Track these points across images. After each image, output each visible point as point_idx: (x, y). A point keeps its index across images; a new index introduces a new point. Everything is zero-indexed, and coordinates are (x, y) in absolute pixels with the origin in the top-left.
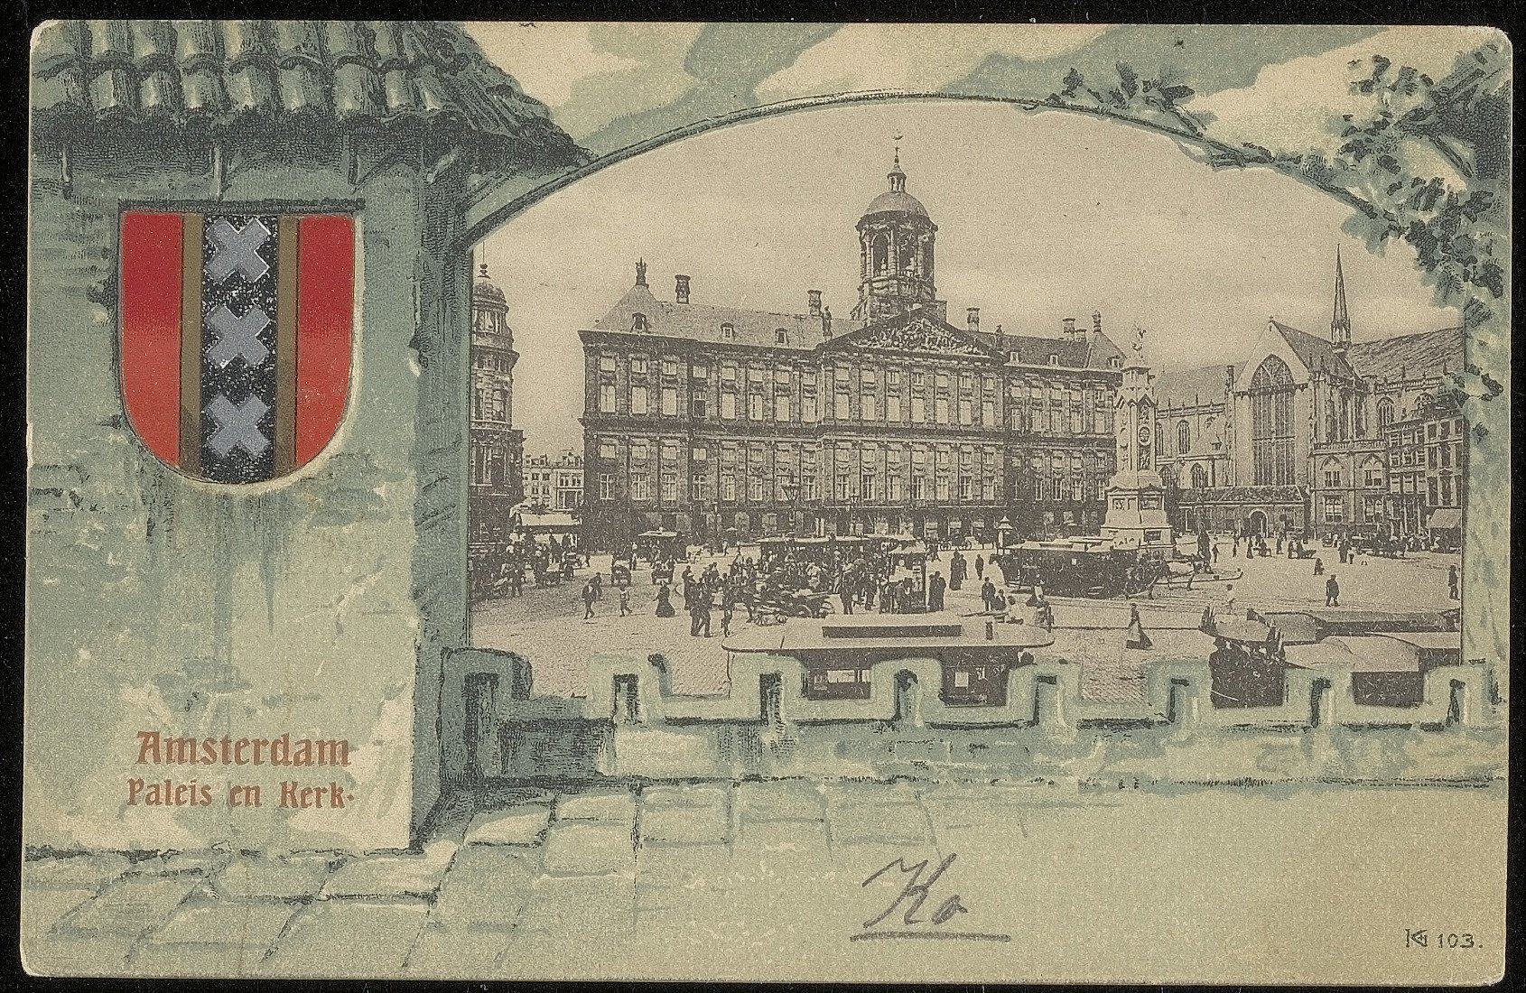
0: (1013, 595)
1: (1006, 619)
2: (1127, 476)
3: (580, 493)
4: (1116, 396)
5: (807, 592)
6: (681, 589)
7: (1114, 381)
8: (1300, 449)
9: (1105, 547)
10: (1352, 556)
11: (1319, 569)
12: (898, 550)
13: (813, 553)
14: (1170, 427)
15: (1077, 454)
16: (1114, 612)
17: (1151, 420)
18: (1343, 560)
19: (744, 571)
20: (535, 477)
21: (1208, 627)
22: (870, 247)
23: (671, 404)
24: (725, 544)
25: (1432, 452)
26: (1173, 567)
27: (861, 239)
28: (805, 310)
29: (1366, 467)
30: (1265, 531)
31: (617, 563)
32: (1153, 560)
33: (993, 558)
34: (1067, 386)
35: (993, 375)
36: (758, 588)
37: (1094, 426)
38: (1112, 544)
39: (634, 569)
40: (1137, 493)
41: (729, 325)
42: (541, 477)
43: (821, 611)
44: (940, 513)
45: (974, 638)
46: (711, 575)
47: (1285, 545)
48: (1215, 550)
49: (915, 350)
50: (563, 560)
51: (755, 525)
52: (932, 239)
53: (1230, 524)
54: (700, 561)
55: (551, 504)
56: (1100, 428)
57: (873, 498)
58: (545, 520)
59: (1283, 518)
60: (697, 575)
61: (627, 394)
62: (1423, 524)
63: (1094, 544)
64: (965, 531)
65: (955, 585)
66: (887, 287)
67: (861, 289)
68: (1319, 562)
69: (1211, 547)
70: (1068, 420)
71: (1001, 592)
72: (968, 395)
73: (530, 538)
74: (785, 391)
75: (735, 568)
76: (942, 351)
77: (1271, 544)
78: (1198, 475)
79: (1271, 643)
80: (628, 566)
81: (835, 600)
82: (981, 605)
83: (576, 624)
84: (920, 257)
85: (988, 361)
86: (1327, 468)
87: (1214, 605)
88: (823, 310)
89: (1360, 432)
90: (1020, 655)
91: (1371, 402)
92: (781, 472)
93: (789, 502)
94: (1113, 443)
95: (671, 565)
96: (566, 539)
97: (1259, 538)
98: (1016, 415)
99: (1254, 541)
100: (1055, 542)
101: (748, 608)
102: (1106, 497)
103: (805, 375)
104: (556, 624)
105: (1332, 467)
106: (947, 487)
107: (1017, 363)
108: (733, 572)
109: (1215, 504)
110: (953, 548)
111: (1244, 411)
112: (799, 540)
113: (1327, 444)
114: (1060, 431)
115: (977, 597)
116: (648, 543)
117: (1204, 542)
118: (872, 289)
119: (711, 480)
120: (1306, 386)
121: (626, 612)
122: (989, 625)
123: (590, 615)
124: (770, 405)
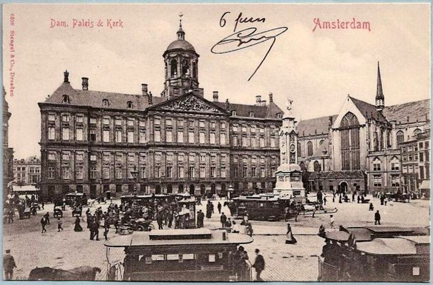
0: (235, 220)
1: (232, 231)
2: (285, 166)
3: (39, 176)
4: (279, 130)
5: (142, 220)
6: (85, 219)
7: (279, 123)
8: (363, 153)
9: (275, 198)
10: (386, 202)
11: (371, 208)
12: (183, 201)
13: (145, 201)
14: (304, 145)
15: (262, 157)
16: (279, 228)
17: (296, 142)
18: (382, 204)
19: (114, 210)
20: (19, 169)
21: (322, 234)
22: (169, 64)
23: (81, 136)
24: (105, 198)
25: (421, 154)
26: (307, 207)
27: (165, 61)
28: (141, 93)
29: (393, 161)
30: (347, 191)
31: (56, 207)
32: (297, 204)
33: (226, 204)
34: (258, 126)
35: (225, 122)
36: (120, 218)
37: (270, 144)
38: (278, 197)
39: (64, 210)
40: (289, 174)
41: (105, 100)
42: (21, 169)
43: (149, 228)
44: (202, 183)
45: (217, 240)
46: (99, 212)
47: (356, 197)
48: (325, 199)
49: (190, 111)
50: (32, 206)
51: (118, 190)
52: (197, 61)
53: (331, 188)
54: (94, 206)
55: (26, 181)
56: (273, 145)
57: (171, 177)
58: (24, 188)
59: (355, 185)
60: (93, 212)
61: (60, 131)
62: (418, 187)
63: (271, 197)
64: (213, 191)
65: (209, 216)
66: (177, 82)
67: (165, 83)
68: (371, 205)
69: (323, 198)
70: (258, 142)
71: (229, 219)
72: (213, 131)
73: (16, 196)
74: (132, 129)
75: (110, 209)
76: (202, 111)
77: (350, 196)
78: (317, 167)
79: (350, 240)
80: (61, 209)
81: (155, 223)
82: (220, 225)
83: (37, 236)
84: (192, 69)
85: (223, 115)
86: (375, 162)
87: (325, 224)
88: (148, 93)
89: (389, 146)
90: (238, 247)
91: (394, 133)
92: (130, 166)
93: (135, 179)
94: (279, 151)
95: (81, 208)
96: (33, 197)
97: (344, 194)
98: (235, 140)
99: (342, 196)
100: (254, 196)
101: (116, 226)
102: (276, 176)
103: (141, 122)
104: (30, 236)
105: (377, 162)
106: (204, 172)
107: (235, 116)
108: (109, 211)
109: (324, 179)
110: (208, 199)
111: (336, 138)
112: (139, 196)
113: (374, 151)
114: (255, 146)
115: (218, 221)
116: (70, 198)
117: (320, 197)
118: (170, 83)
119: (98, 170)
120: (364, 125)
121: (60, 229)
122: (224, 234)
123: (44, 231)
124: (125, 135)
